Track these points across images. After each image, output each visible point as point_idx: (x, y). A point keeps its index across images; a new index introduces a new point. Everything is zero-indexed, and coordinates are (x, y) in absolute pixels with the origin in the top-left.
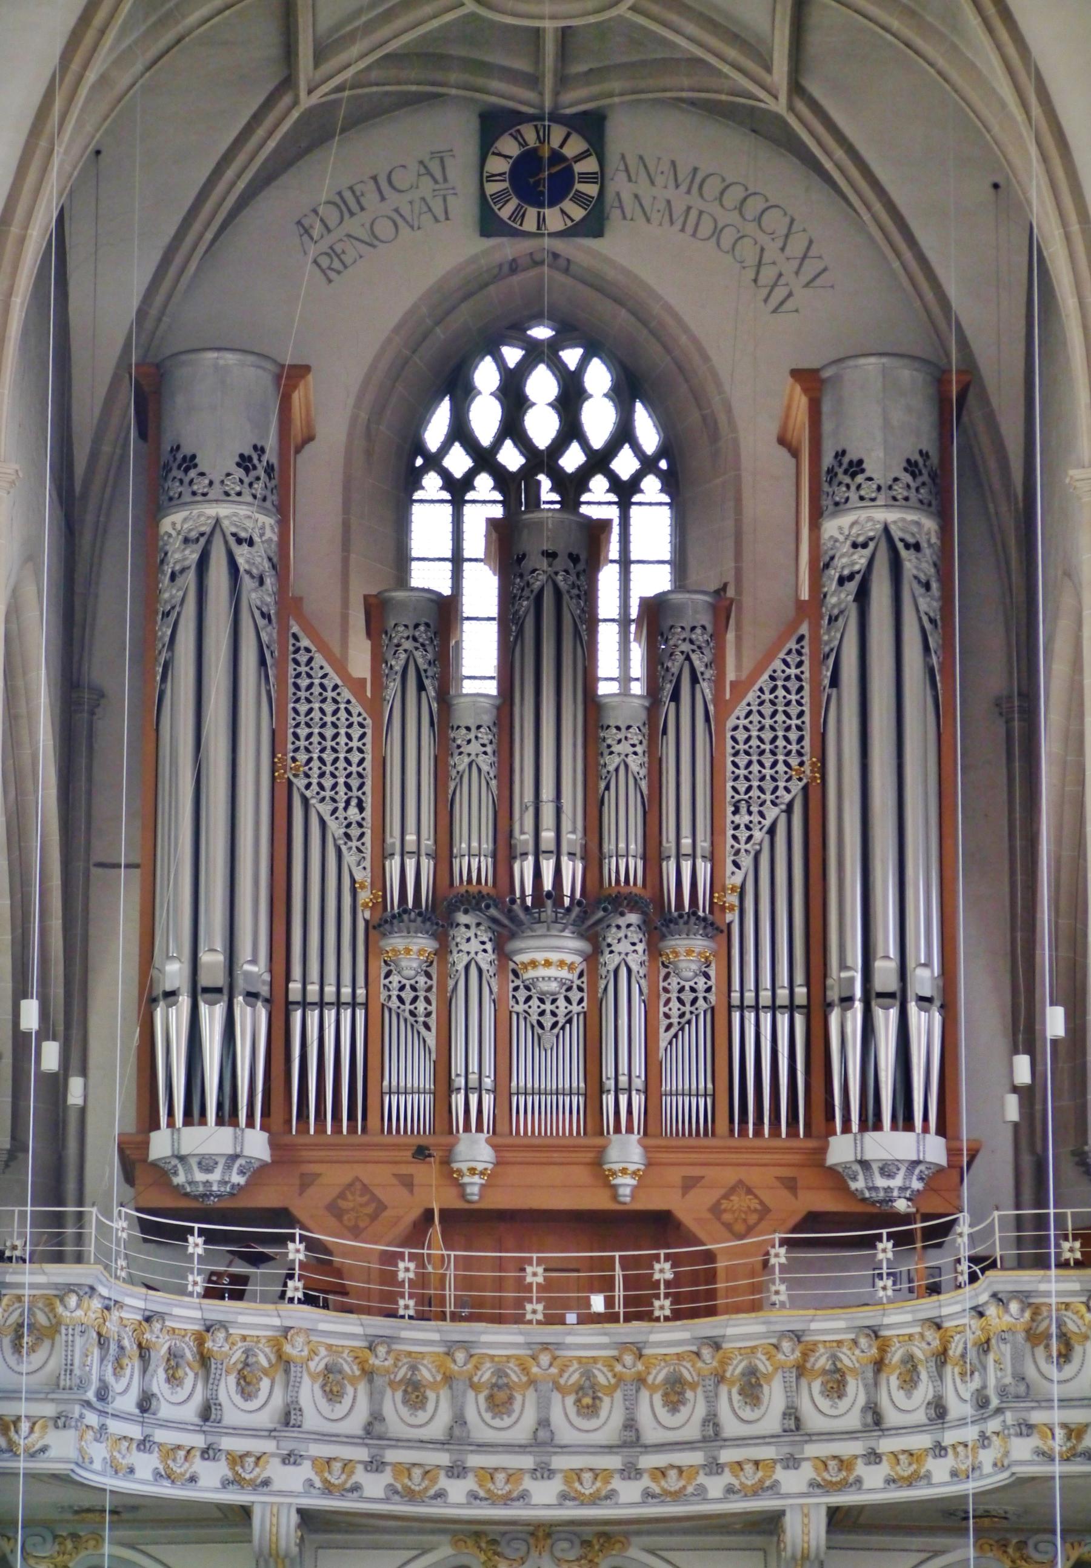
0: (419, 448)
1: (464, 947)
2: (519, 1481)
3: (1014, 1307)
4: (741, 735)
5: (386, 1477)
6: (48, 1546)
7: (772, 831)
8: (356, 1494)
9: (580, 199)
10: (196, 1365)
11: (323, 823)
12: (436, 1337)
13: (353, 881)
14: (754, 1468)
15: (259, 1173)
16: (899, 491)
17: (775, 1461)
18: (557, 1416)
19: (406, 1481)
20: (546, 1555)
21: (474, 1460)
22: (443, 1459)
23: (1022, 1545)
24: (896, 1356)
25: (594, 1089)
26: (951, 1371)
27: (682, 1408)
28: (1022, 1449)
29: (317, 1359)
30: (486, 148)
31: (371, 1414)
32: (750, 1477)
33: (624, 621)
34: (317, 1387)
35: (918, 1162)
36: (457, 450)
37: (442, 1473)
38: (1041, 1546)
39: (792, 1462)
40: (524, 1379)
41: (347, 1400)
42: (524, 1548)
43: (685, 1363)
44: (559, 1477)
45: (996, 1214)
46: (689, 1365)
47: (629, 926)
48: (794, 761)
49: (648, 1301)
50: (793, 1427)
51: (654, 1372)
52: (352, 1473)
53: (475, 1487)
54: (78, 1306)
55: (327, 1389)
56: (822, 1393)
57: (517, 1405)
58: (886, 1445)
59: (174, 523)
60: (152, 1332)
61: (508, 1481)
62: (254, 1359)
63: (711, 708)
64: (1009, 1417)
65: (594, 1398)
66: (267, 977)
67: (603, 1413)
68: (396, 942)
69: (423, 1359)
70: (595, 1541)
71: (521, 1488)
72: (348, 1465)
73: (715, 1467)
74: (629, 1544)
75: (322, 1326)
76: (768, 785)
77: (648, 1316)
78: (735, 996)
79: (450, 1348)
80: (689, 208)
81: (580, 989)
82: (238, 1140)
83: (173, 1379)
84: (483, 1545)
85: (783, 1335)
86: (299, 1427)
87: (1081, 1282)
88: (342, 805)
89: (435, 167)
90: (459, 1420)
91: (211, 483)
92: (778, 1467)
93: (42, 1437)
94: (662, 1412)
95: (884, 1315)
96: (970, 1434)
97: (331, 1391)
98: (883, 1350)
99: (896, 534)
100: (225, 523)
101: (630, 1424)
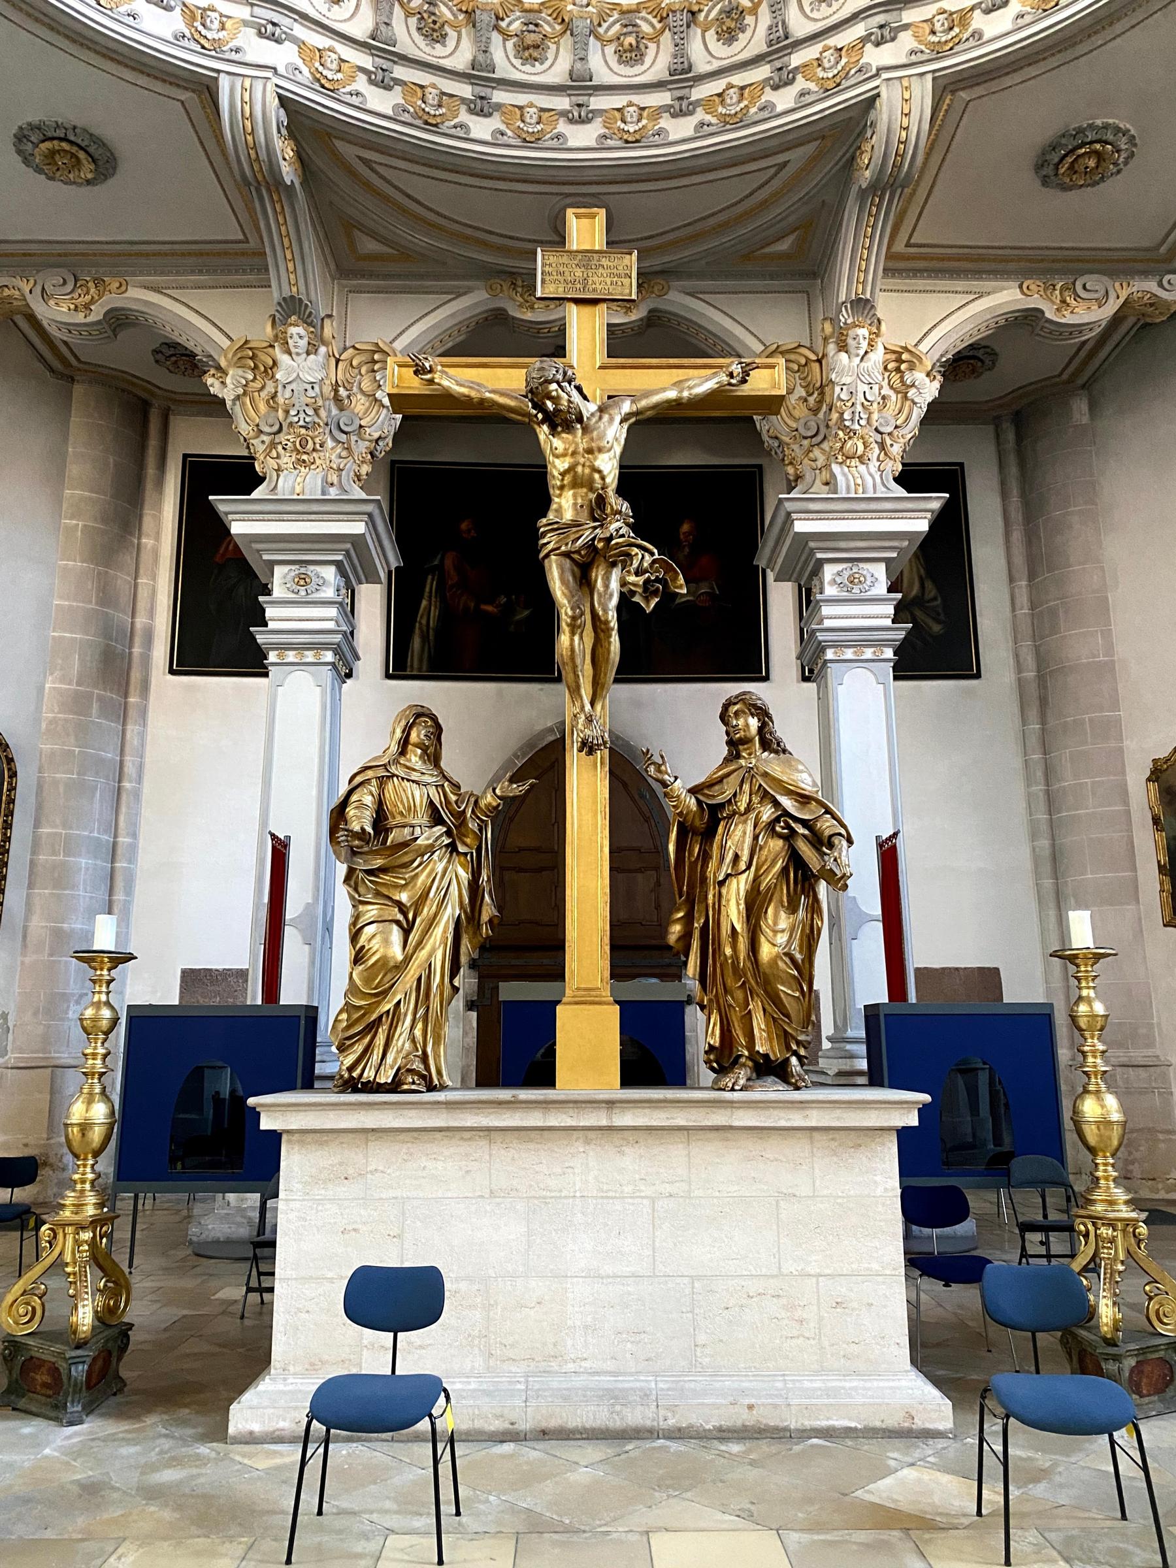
6: (69, 287)
17: (864, 40)
19: (419, 102)
22: (465, 90)
27: (741, 35)
31: (377, 24)
38: (1088, 287)
40: (558, 27)
53: (503, 127)
57: (550, 54)
65: (638, 42)
67: (648, 60)
74: (669, 288)
84: (520, 290)
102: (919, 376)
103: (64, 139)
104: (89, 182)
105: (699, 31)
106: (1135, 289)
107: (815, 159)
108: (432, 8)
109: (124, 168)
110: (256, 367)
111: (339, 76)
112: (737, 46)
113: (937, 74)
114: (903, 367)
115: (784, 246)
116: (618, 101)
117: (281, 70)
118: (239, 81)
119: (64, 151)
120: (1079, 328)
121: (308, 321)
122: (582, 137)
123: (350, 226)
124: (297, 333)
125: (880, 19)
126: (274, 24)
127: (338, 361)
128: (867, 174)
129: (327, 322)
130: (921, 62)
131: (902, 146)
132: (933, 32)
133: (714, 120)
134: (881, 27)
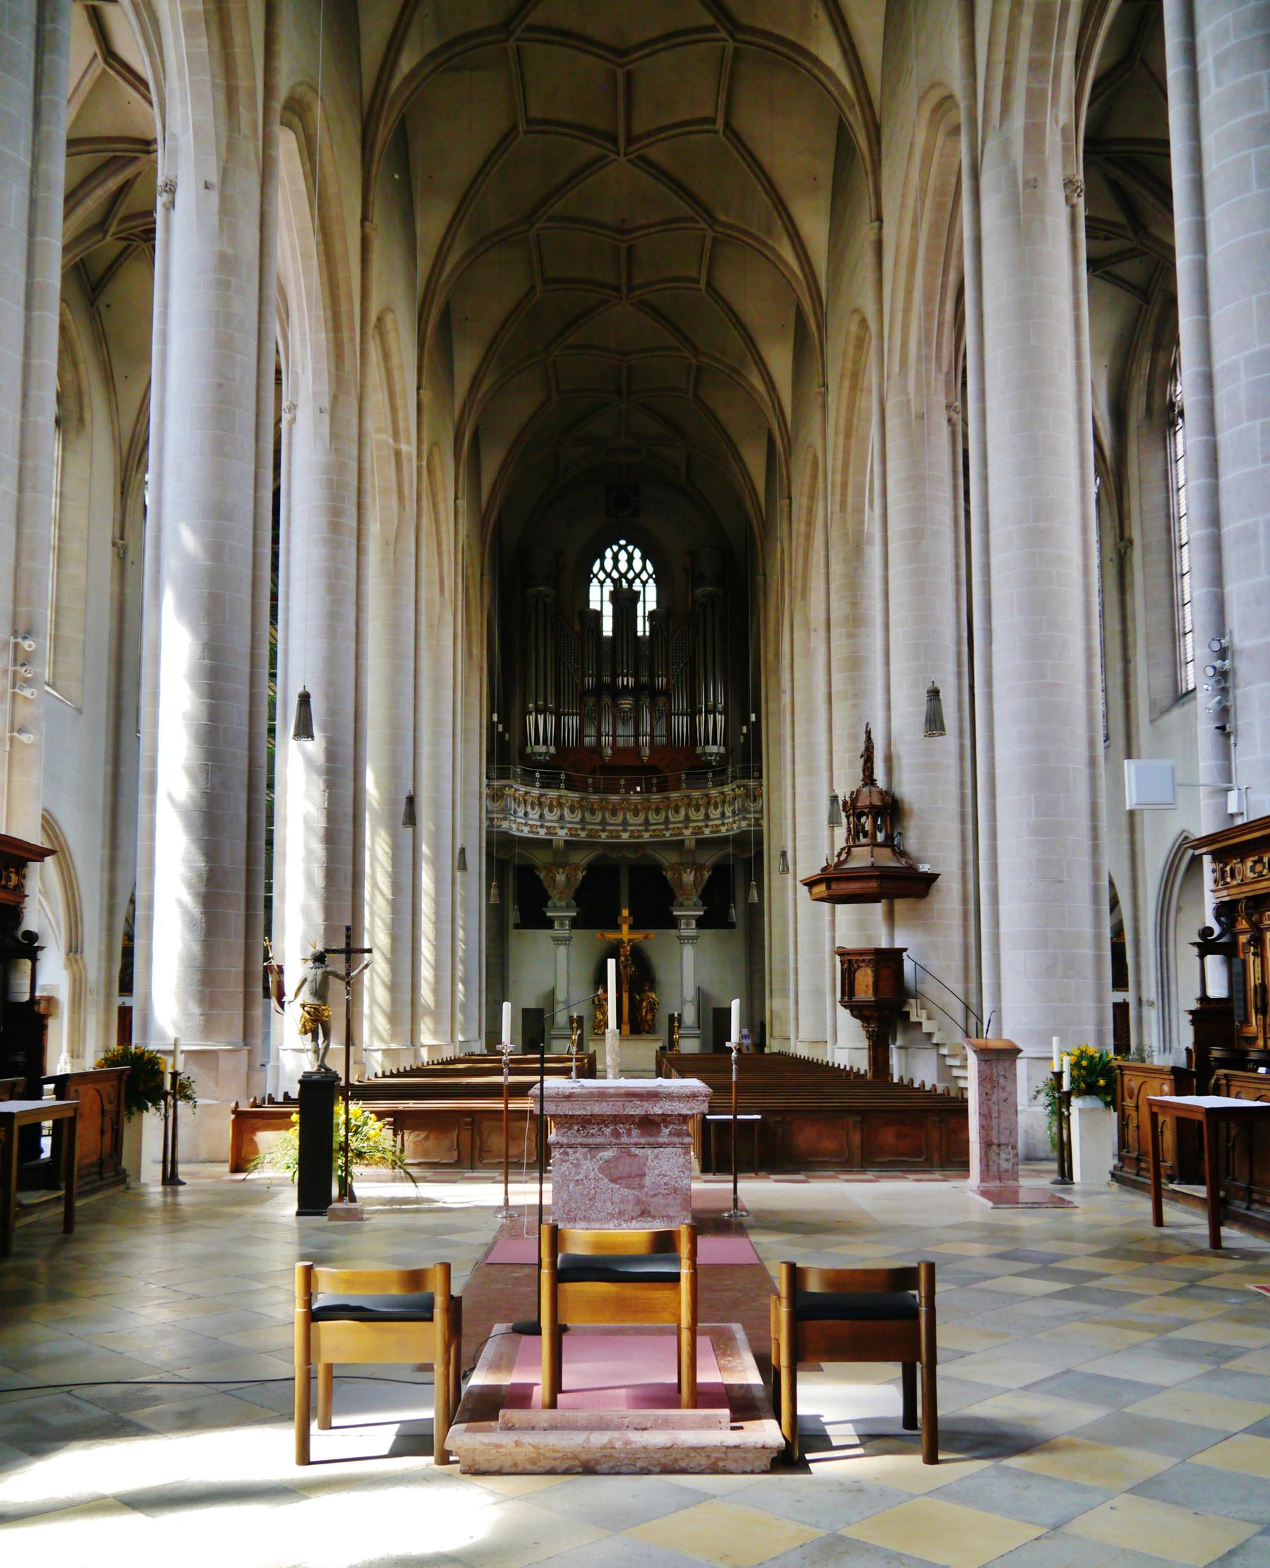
0: (592, 572)
15: (552, 756)
18: (628, 816)
21: (608, 828)
22: (600, 827)
24: (713, 801)
25: (637, 735)
26: (726, 806)
28: (744, 824)
32: (677, 832)
33: (644, 617)
35: (717, 754)
36: (601, 572)
39: (686, 828)
49: (651, 788)
58: (710, 823)
59: (531, 591)
72: (576, 829)
73: (667, 829)
77: (651, 792)
79: (601, 800)
82: (548, 749)
83: (533, 808)
90: (604, 817)
96: (731, 820)
102: (706, 872)
121: (562, 867)
122: (625, 836)
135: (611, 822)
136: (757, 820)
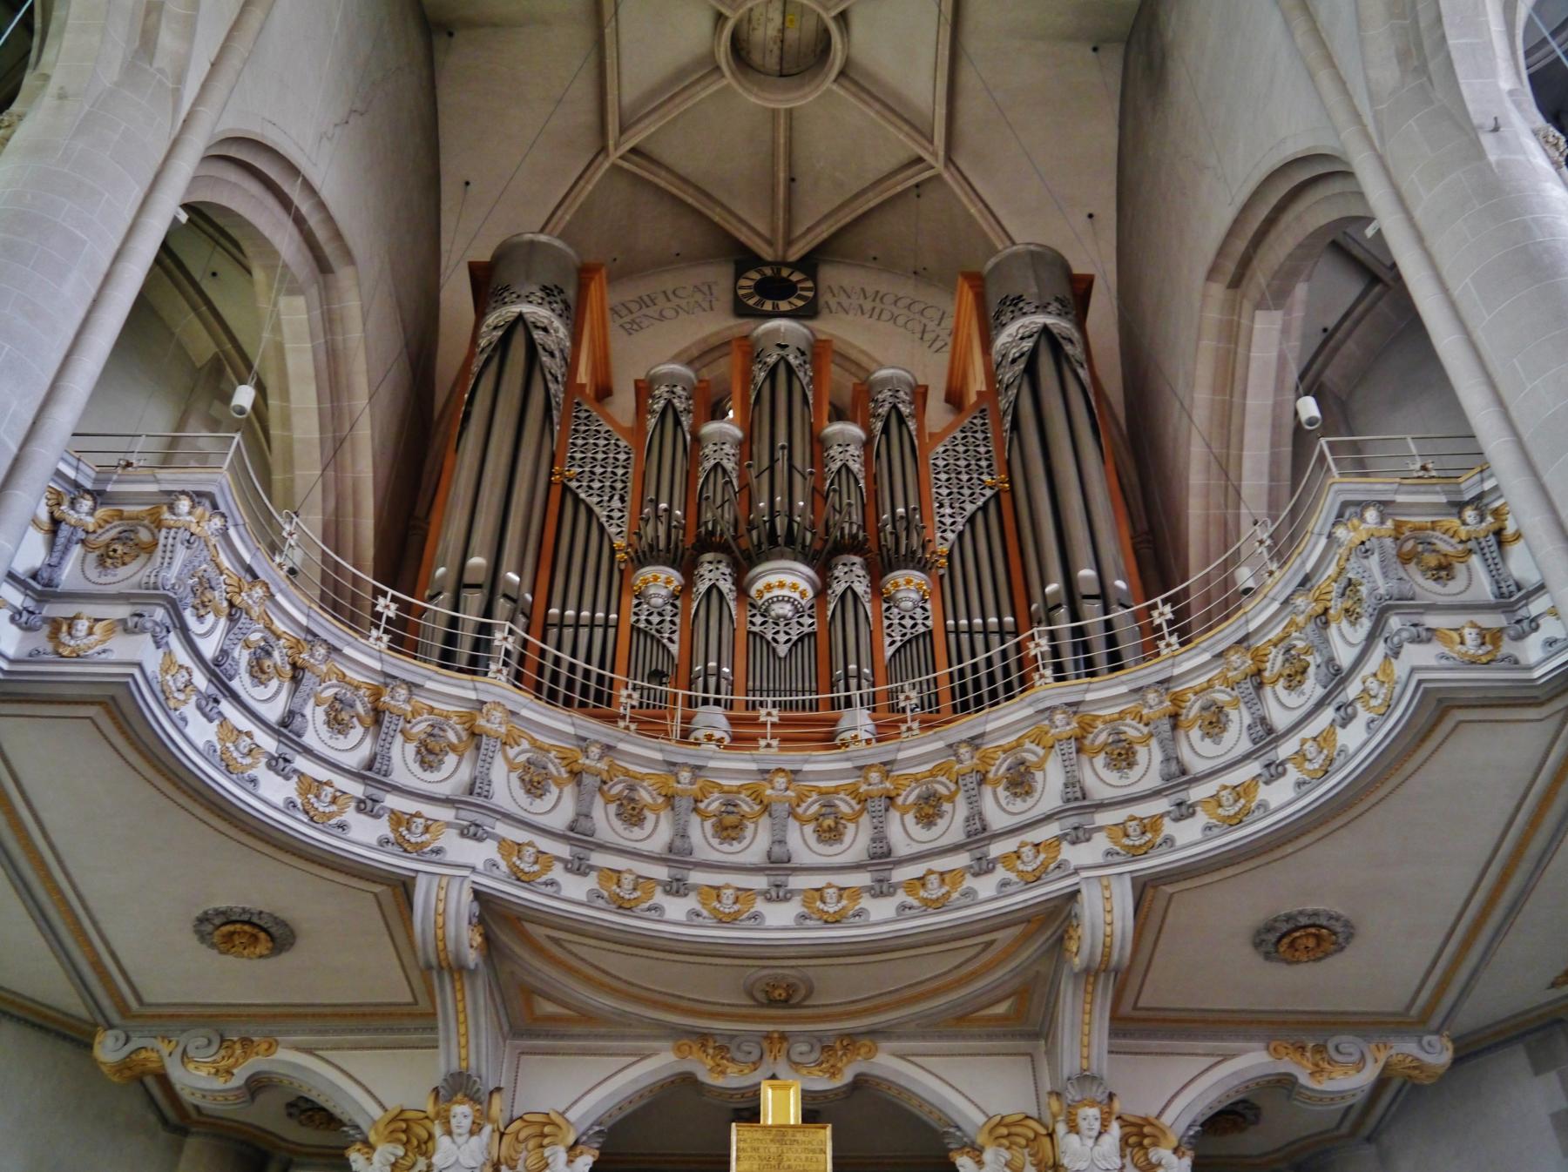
1: (708, 575)
2: (752, 902)
3: (1371, 515)
4: (941, 463)
5: (591, 882)
7: (971, 520)
8: (550, 890)
9: (800, 297)
10: (368, 721)
11: (590, 511)
12: (659, 756)
13: (611, 543)
14: (1033, 851)
16: (1051, 308)
17: (1060, 839)
19: (615, 887)
20: (782, 1060)
21: (696, 877)
22: (661, 872)
23: (1320, 1049)
24: (1193, 708)
29: (517, 749)
30: (738, 276)
31: (578, 815)
32: (1030, 864)
34: (514, 776)
37: (659, 890)
38: (1341, 1048)
39: (1079, 836)
40: (757, 808)
41: (550, 798)
42: (755, 1056)
43: (939, 778)
44: (797, 900)
45: (1323, 441)
46: (944, 779)
47: (854, 564)
48: (985, 477)
50: (1079, 794)
51: (904, 793)
52: (548, 868)
53: (698, 907)
54: (190, 513)
55: (527, 778)
56: (1107, 766)
57: (749, 832)
60: (312, 656)
61: (736, 901)
62: (441, 733)
63: (916, 442)
64: (1394, 622)
65: (837, 823)
66: (529, 597)
67: (848, 839)
68: (648, 572)
69: (643, 780)
70: (838, 1045)
71: (752, 910)
73: (983, 867)
75: (525, 713)
76: (966, 492)
78: (951, 622)
80: (874, 309)
81: (811, 616)
84: (711, 1051)
85: (1052, 709)
86: (486, 797)
87: (1446, 493)
88: (606, 498)
89: (705, 289)
91: (519, 297)
92: (1065, 845)
93: (104, 641)
94: (917, 831)
95: (1173, 665)
97: (531, 781)
98: (1177, 700)
99: (1055, 331)
100: (526, 316)
101: (879, 837)
103: (249, 923)
104: (261, 956)
105: (897, 814)
106: (1393, 1052)
107: (1026, 938)
108: (631, 795)
109: (301, 943)
110: (408, 1141)
111: (536, 868)
112: (936, 831)
113: (1135, 875)
114: (1146, 1142)
115: (1001, 1009)
116: (817, 881)
117: (480, 867)
118: (436, 880)
119: (245, 932)
120: (1342, 1095)
121: (473, 1098)
123: (529, 993)
124: (462, 1113)
125: (1074, 821)
126: (477, 825)
127: (502, 1135)
128: (1077, 960)
129: (496, 1099)
130: (1119, 864)
131: (1108, 939)
132: (1127, 835)
133: (916, 903)
134: (1076, 829)
135: (715, 857)
136: (1490, 637)
